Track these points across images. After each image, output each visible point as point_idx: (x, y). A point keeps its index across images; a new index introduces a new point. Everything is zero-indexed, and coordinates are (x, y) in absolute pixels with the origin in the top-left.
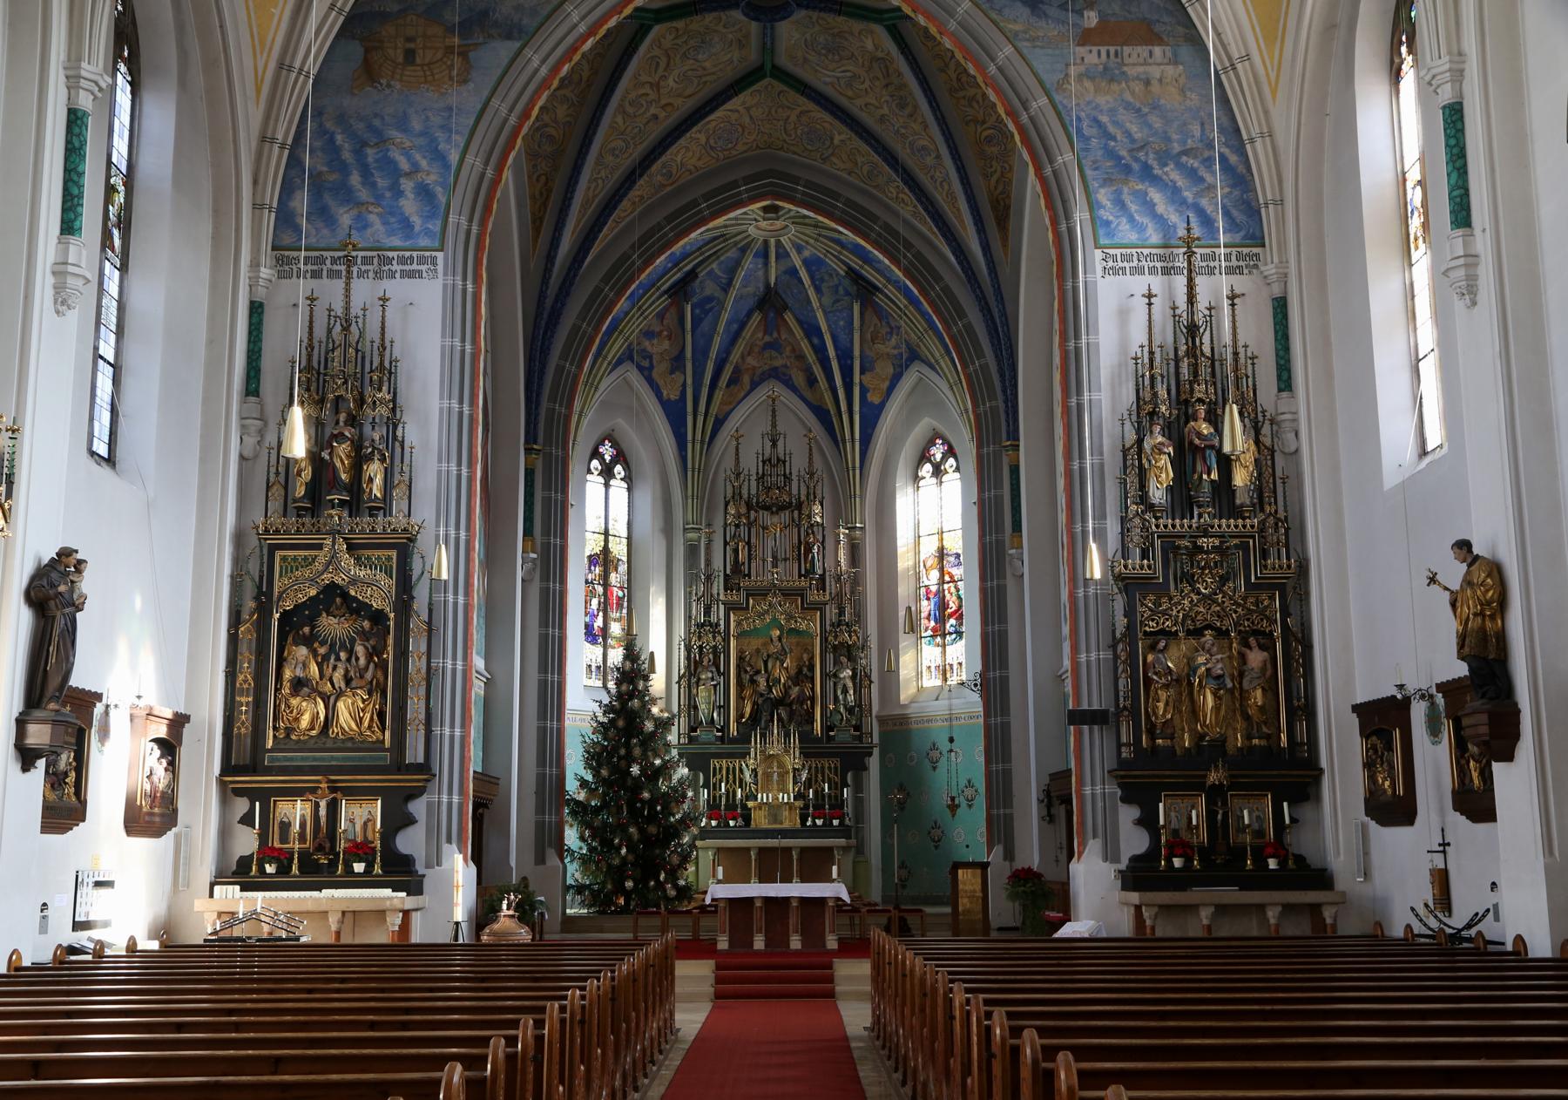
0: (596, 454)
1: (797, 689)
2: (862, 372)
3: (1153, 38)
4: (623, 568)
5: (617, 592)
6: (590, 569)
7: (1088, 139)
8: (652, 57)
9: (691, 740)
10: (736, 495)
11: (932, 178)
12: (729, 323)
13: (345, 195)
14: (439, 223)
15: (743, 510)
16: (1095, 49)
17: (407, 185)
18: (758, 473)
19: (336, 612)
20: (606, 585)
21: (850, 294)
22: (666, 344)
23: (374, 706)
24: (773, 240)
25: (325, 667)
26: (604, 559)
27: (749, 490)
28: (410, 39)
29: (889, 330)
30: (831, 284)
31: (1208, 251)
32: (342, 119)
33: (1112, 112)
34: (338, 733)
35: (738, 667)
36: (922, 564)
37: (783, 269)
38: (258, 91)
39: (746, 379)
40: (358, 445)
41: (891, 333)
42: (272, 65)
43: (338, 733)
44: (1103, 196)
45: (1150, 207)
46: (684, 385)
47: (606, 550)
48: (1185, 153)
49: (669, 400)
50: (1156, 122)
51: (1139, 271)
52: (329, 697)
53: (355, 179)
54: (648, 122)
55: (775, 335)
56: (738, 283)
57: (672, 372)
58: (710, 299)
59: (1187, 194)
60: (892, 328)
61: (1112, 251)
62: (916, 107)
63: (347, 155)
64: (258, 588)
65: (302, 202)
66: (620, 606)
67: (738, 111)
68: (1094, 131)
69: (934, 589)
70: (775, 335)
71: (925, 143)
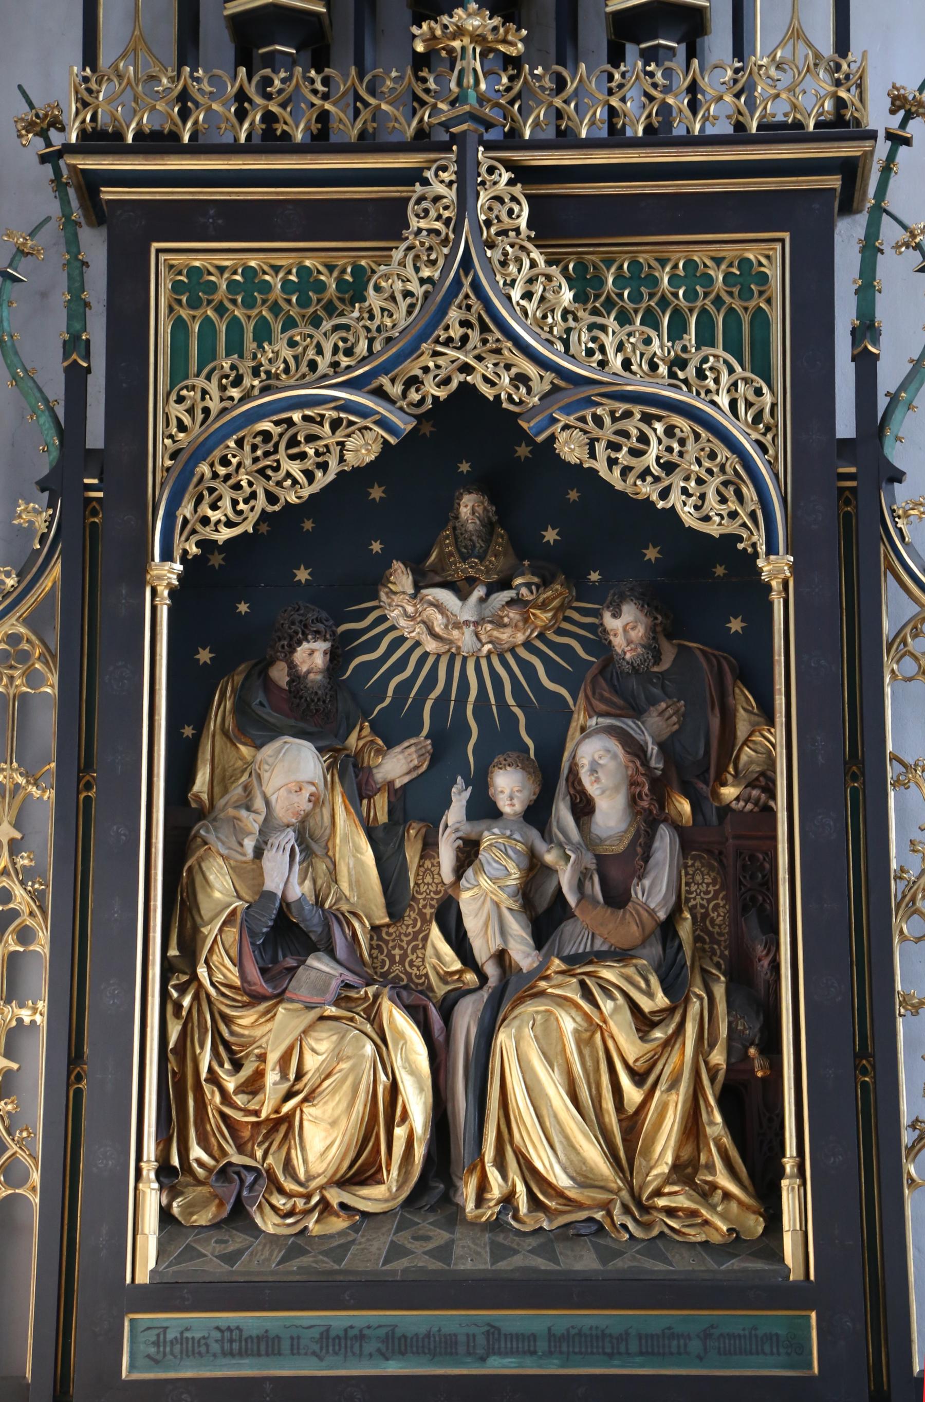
19: (461, 569)
23: (703, 1045)
25: (412, 854)
34: (508, 1200)
43: (508, 1200)
52: (447, 1009)
64: (61, 433)
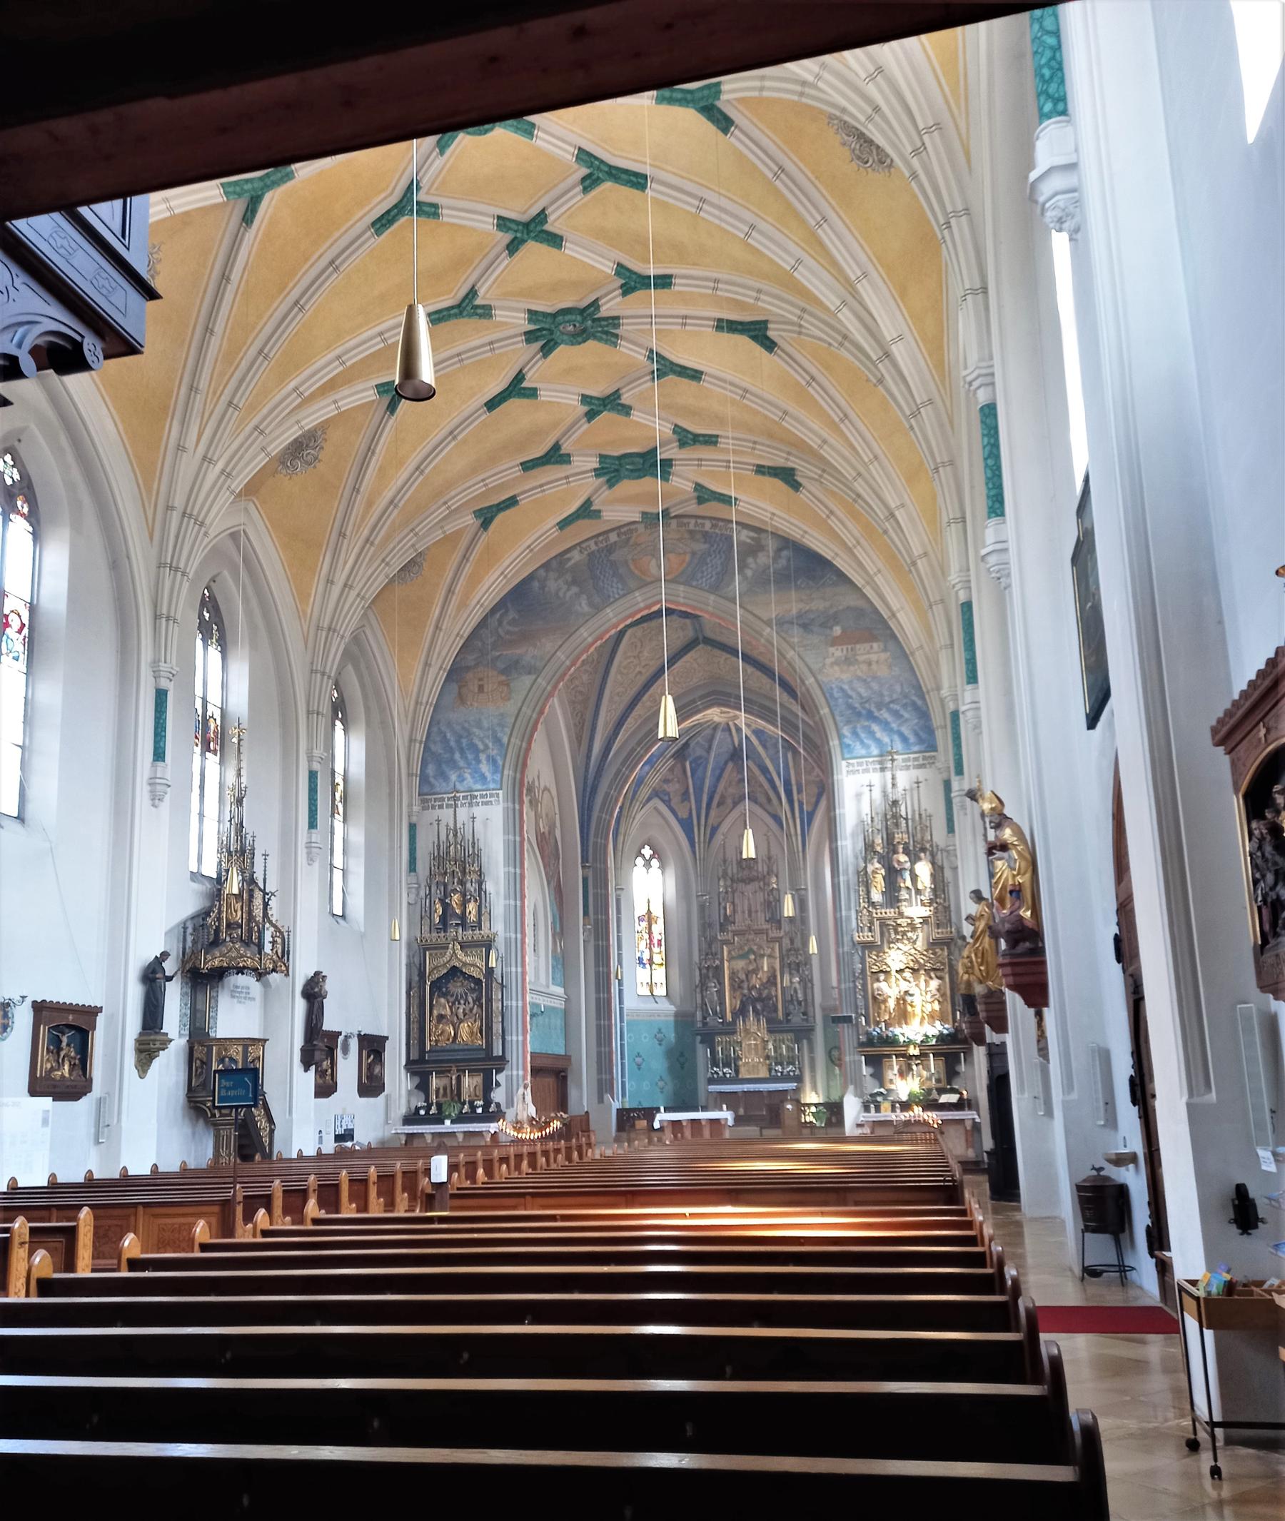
0: (640, 854)
1: (766, 991)
3: (873, 638)
4: (661, 921)
5: (656, 937)
7: (837, 699)
9: (705, 1024)
10: (725, 875)
12: (713, 770)
13: (453, 764)
14: (499, 775)
15: (729, 883)
16: (840, 648)
17: (483, 757)
20: (650, 933)
22: (677, 786)
24: (731, 723)
26: (649, 917)
28: (481, 679)
31: (906, 756)
32: (449, 724)
33: (850, 682)
35: (731, 978)
38: (407, 717)
39: (729, 801)
40: (464, 895)
42: (413, 703)
44: (846, 731)
45: (872, 734)
46: (691, 810)
47: (649, 912)
48: (892, 702)
50: (875, 686)
51: (866, 771)
53: (457, 756)
56: (714, 747)
57: (683, 801)
58: (700, 757)
59: (894, 726)
61: (851, 761)
63: (452, 744)
65: (431, 770)
66: (660, 944)
68: (840, 694)
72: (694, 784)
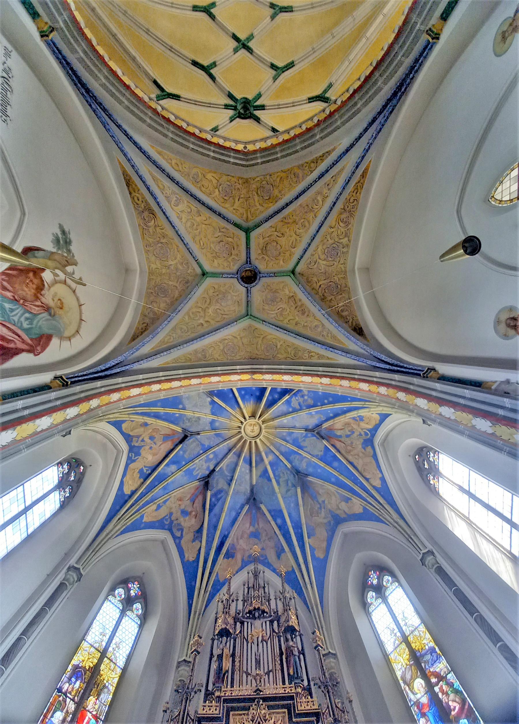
2: (309, 538)
4: (107, 697)
6: (70, 679)
8: (204, 297)
11: (323, 335)
12: (230, 509)
15: (231, 621)
18: (244, 595)
21: (294, 486)
22: (193, 520)
27: (236, 607)
29: (319, 506)
30: (284, 479)
36: (401, 682)
37: (259, 474)
41: (320, 508)
47: (96, 670)
49: (188, 561)
54: (198, 326)
55: (256, 526)
57: (194, 541)
58: (220, 491)
60: (319, 504)
62: (309, 311)
67: (237, 338)
69: (424, 700)
70: (256, 526)
71: (316, 323)
72: (209, 521)
